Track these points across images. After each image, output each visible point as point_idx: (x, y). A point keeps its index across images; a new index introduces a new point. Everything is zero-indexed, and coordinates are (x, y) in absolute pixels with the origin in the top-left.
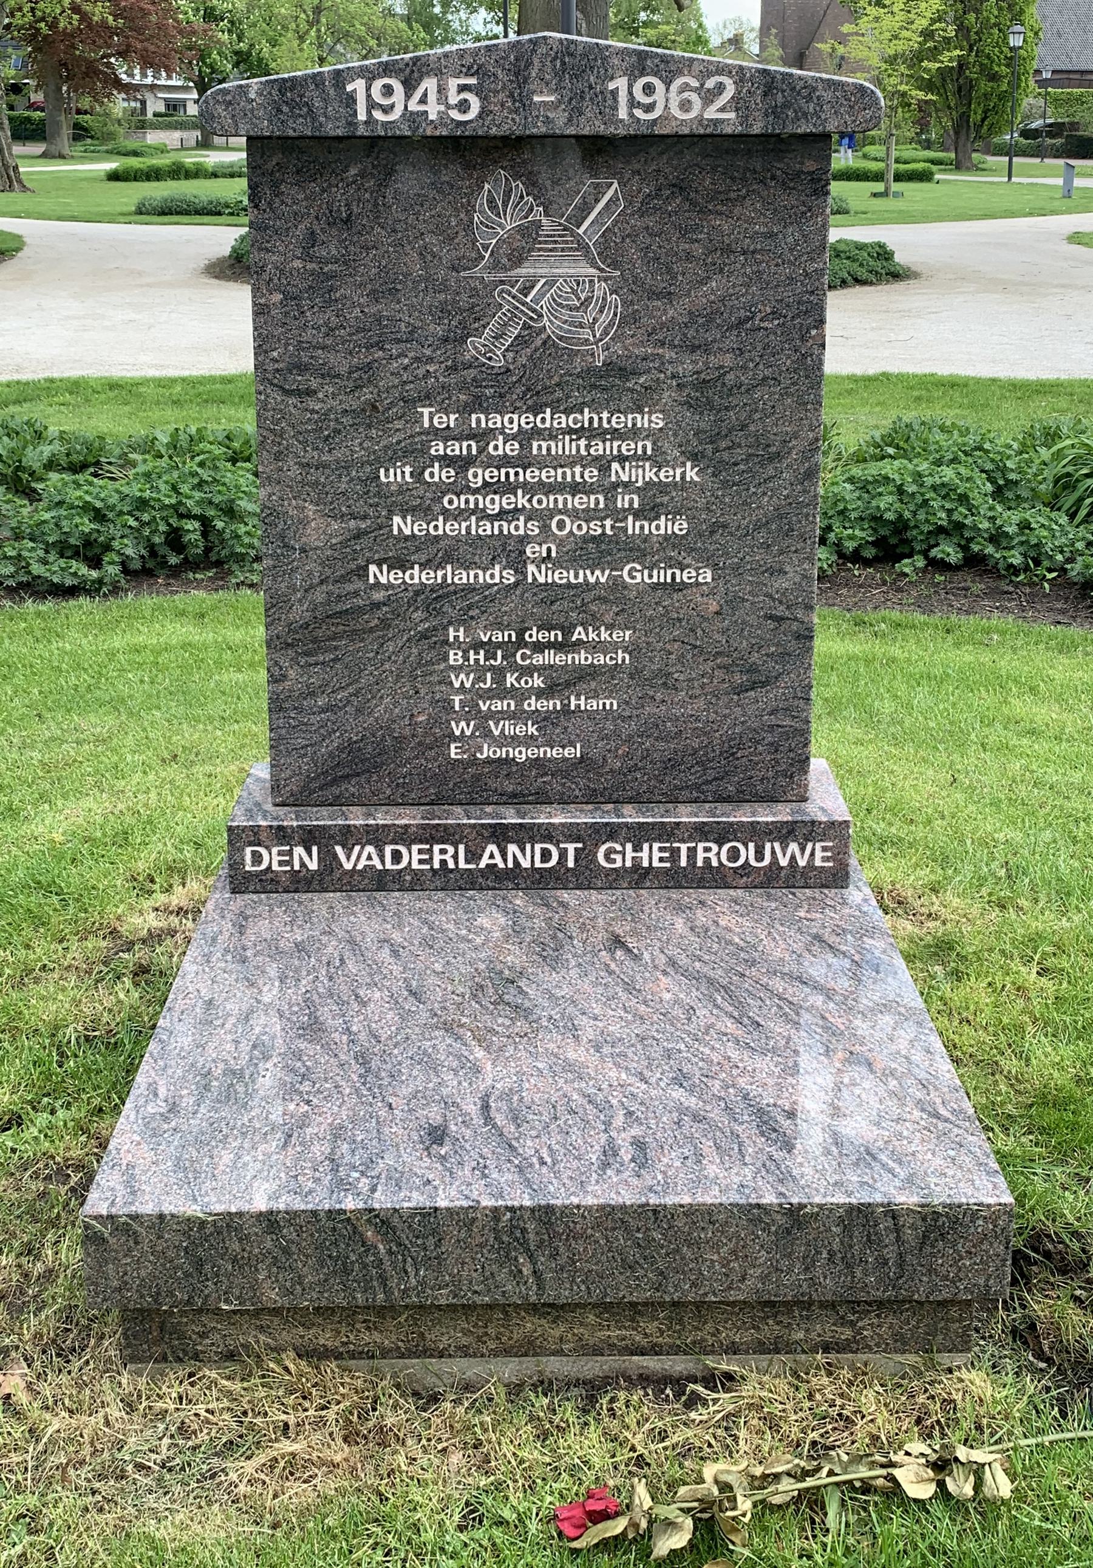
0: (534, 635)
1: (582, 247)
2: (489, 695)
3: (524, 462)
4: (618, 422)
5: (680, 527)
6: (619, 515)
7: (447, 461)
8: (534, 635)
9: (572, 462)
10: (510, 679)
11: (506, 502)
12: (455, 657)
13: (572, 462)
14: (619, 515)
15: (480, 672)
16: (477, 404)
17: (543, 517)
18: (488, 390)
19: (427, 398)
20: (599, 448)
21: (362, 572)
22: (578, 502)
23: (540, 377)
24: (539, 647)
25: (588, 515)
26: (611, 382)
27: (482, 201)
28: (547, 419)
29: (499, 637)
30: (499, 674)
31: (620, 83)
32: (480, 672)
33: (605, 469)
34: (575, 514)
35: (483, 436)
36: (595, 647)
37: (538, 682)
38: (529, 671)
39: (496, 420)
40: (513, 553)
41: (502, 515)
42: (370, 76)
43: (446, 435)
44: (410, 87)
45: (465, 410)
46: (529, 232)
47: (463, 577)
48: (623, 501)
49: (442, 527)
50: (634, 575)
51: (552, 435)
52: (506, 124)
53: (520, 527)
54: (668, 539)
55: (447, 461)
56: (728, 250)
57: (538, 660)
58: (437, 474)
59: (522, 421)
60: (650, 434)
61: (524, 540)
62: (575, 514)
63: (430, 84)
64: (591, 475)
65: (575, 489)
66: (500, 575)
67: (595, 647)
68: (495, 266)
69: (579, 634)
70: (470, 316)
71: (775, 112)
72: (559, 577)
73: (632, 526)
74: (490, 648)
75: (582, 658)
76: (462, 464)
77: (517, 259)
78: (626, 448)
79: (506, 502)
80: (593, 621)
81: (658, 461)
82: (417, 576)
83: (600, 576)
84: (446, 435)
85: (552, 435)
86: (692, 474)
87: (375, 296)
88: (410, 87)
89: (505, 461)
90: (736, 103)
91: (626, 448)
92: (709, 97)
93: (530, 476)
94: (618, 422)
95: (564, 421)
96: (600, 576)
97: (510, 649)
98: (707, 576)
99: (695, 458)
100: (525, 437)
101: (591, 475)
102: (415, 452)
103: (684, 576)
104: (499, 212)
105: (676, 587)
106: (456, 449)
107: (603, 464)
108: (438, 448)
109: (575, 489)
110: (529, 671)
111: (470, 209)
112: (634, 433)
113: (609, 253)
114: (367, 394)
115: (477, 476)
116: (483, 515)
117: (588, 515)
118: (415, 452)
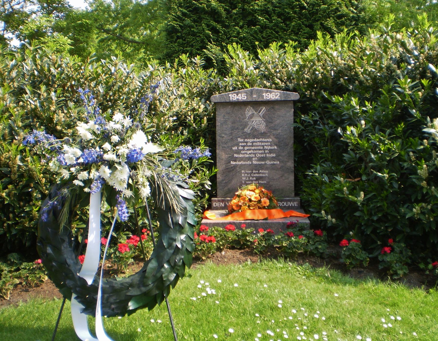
0: (254, 172)
1: (260, 116)
2: (248, 181)
3: (252, 146)
4: (265, 140)
5: (274, 155)
6: (266, 154)
7: (242, 146)
8: (254, 172)
9: (259, 146)
10: (251, 178)
11: (250, 152)
12: (243, 175)
13: (259, 146)
14: (266, 154)
15: (246, 177)
16: (246, 138)
17: (255, 154)
18: (247, 136)
19: (239, 137)
20: (263, 144)
21: (230, 162)
22: (260, 152)
23: (256, 134)
24: (255, 173)
25: (261, 154)
26: (264, 135)
27: (247, 110)
28: (256, 140)
29: (249, 172)
30: (249, 177)
31: (264, 94)
32: (246, 177)
33: (264, 147)
34: (260, 153)
35: (247, 142)
36: (263, 173)
37: (255, 179)
38: (253, 177)
39: (249, 140)
40: (250, 159)
41: (250, 154)
42: (232, 94)
43: (242, 142)
44: (237, 95)
45: (244, 139)
46: (253, 114)
47: (244, 163)
48: (266, 152)
49: (241, 156)
50: (268, 162)
51: (256, 142)
52: (250, 99)
53: (252, 155)
54: (273, 157)
55: (242, 146)
56: (280, 116)
57: (255, 175)
58: (240, 148)
59: (253, 140)
60: (270, 142)
61: (253, 157)
62: (260, 153)
63: (240, 95)
64: (262, 148)
65: (260, 150)
66: (249, 163)
67: (263, 173)
68: (248, 119)
69: (260, 171)
70: (246, 125)
71: (285, 97)
72: (258, 163)
73: (268, 155)
74: (248, 173)
75: (261, 175)
76: (244, 146)
77: (251, 118)
78: (267, 144)
79: (250, 152)
80: (262, 169)
81: (271, 146)
82: (238, 163)
83: (263, 163)
84: (242, 142)
85: (256, 142)
86: (276, 148)
87: (232, 123)
88: (237, 95)
89: (250, 146)
90: (280, 96)
91: (267, 144)
92: (276, 96)
93: (253, 148)
94: (265, 140)
95: (258, 140)
96: (263, 163)
97: (251, 173)
98: (278, 163)
99: (276, 145)
100: (252, 142)
101: (262, 148)
102: (238, 145)
103: (275, 163)
104: (249, 111)
105: (274, 164)
106: (243, 144)
107: (263, 146)
108: (241, 144)
109: (260, 150)
110: (253, 177)
111: (245, 111)
112: (268, 142)
113: (264, 117)
114: (231, 137)
115: (246, 148)
116: (246, 153)
117: (261, 154)
118: (238, 145)
